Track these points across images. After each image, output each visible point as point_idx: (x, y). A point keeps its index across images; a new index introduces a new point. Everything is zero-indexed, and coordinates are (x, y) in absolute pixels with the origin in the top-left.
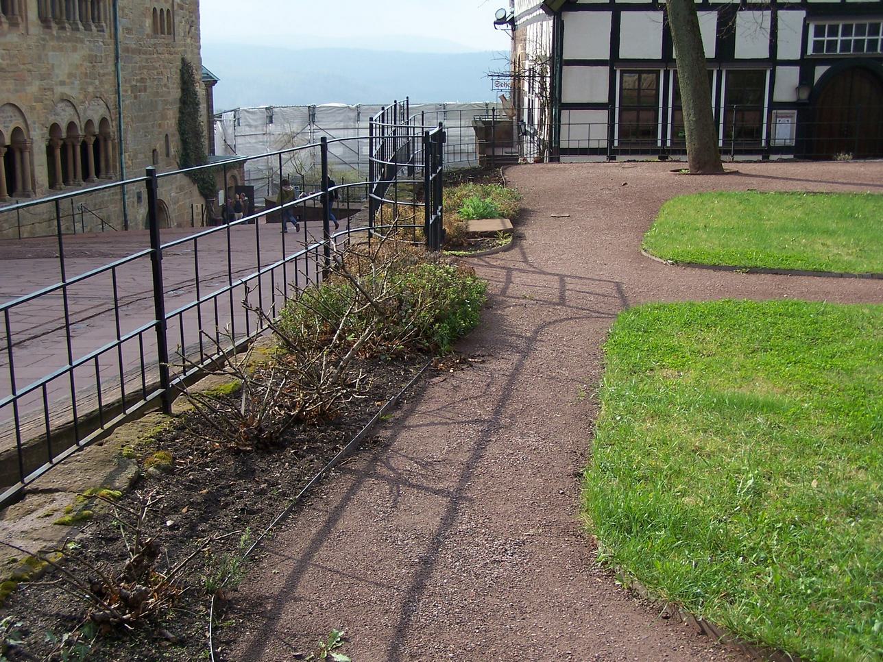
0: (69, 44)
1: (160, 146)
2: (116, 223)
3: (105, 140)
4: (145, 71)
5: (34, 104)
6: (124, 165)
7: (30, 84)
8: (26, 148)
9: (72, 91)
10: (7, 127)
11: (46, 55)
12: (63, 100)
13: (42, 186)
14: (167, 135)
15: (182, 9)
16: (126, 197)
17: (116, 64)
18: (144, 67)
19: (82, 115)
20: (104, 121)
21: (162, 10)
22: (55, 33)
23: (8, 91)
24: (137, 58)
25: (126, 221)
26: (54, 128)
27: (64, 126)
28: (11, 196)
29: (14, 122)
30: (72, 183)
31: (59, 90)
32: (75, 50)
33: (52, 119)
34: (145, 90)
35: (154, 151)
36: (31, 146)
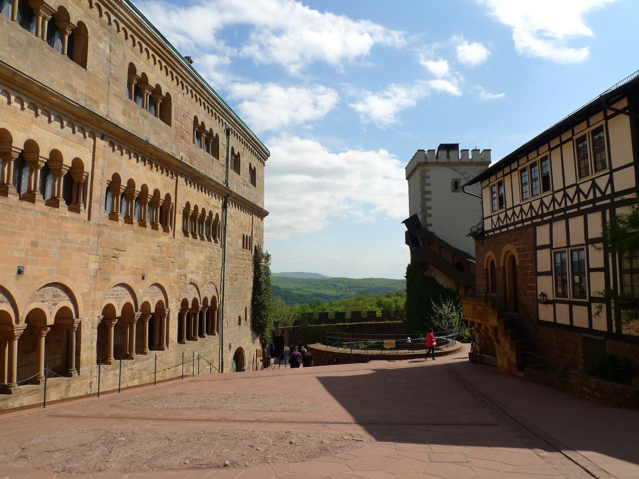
0: (199, 248)
2: (216, 364)
5: (174, 285)
7: (173, 271)
9: (197, 278)
10: (154, 300)
11: (184, 253)
12: (191, 283)
13: (173, 341)
15: (256, 237)
16: (224, 346)
21: (247, 236)
22: (190, 239)
23: (157, 274)
28: (150, 350)
29: (158, 296)
31: (189, 276)
32: (201, 252)
33: (184, 296)
34: (237, 280)
35: (240, 318)
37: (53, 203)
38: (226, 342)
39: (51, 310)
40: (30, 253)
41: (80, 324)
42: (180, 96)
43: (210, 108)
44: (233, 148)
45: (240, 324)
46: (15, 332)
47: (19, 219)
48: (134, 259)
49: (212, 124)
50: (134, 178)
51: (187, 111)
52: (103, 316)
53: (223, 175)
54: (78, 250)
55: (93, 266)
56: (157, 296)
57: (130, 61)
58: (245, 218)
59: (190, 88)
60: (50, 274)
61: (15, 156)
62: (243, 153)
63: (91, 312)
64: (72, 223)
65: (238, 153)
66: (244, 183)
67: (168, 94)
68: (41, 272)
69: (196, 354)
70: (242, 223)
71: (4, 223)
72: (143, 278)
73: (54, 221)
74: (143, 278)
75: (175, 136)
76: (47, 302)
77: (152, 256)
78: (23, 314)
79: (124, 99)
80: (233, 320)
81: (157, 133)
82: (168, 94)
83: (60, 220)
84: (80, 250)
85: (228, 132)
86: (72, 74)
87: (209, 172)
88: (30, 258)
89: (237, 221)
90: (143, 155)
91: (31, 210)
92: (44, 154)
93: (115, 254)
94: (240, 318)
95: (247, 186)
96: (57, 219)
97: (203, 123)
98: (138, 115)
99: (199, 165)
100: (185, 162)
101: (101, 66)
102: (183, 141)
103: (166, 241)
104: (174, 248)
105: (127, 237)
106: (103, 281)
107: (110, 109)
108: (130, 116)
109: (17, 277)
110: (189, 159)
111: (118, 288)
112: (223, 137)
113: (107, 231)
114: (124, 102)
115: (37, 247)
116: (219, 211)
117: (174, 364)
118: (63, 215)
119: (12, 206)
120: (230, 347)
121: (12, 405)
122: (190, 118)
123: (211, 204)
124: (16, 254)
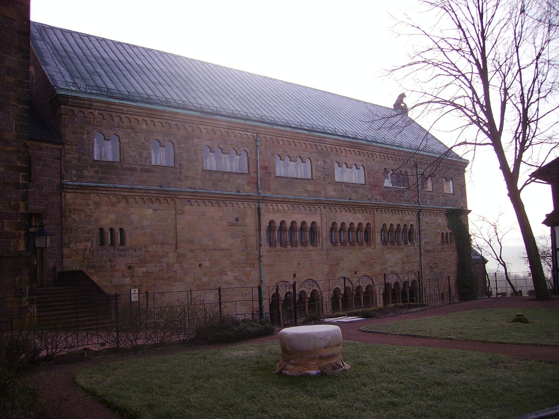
9: (397, 269)
17: (420, 258)
18: (436, 258)
20: (414, 282)
31: (390, 269)
50: (344, 221)
55: (326, 270)
68: (302, 276)
72: (355, 273)
74: (355, 273)
116: (414, 223)
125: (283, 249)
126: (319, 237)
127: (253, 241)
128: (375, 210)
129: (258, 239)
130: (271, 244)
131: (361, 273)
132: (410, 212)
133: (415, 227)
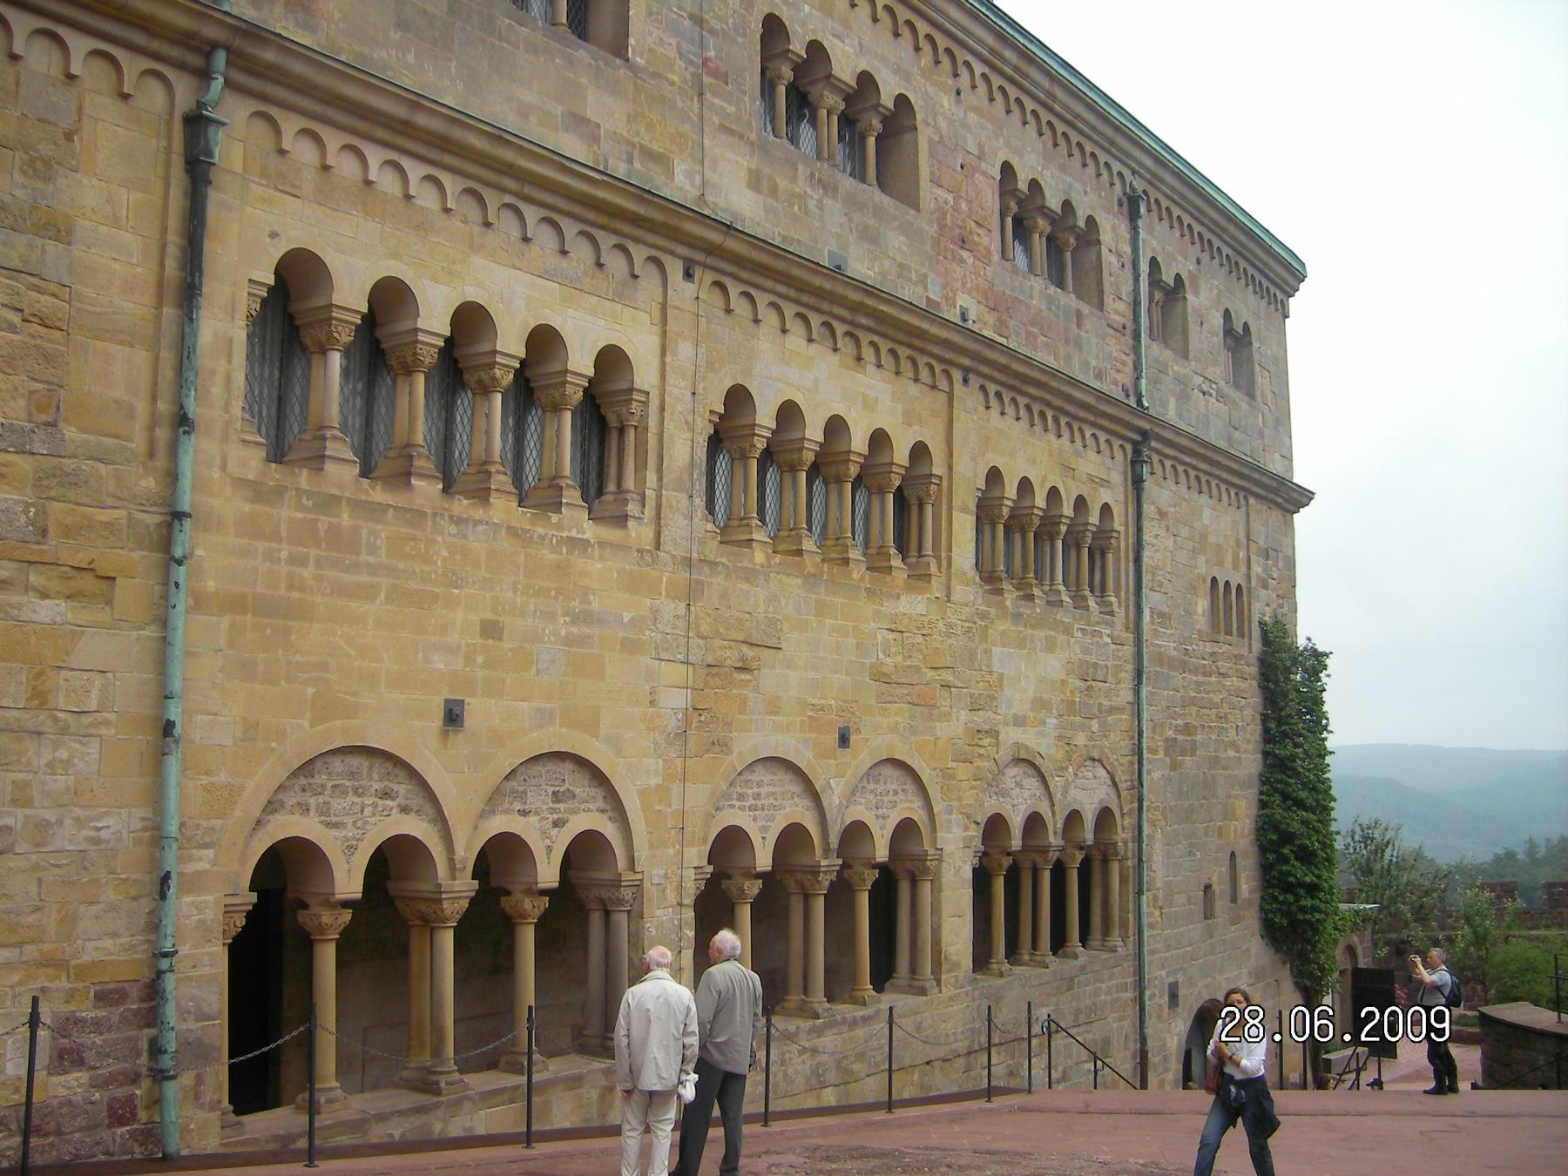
0: (1040, 634)
1: (1218, 876)
2: (1123, 1059)
3: (1105, 861)
4: (1194, 710)
6: (1145, 921)
7: (947, 717)
8: (926, 870)
9: (1041, 742)
10: (884, 818)
12: (1018, 761)
13: (957, 965)
14: (1233, 853)
15: (1266, 587)
16: (1147, 994)
17: (1137, 690)
19: (1058, 797)
20: (1105, 816)
21: (1227, 584)
23: (894, 729)
24: (1178, 678)
25: (1143, 1055)
26: (995, 826)
27: (1016, 822)
29: (900, 807)
30: (1026, 957)
31: (1011, 735)
32: (1050, 646)
33: (991, 805)
35: (1207, 888)
36: (938, 867)
37: (538, 496)
38: (1158, 976)
39: (548, 842)
40: (480, 659)
41: (638, 887)
42: (946, 101)
43: (1060, 127)
44: (1154, 263)
45: (1208, 914)
46: (445, 905)
47: (445, 554)
48: (811, 674)
49: (1062, 183)
50: (799, 398)
51: (974, 149)
52: (710, 869)
53: (1124, 364)
54: (622, 645)
55: (675, 701)
56: (894, 804)
57: (766, 11)
58: (1216, 518)
59: (979, 68)
60: (540, 726)
61: (429, 357)
62: (1194, 279)
63: (671, 851)
64: (602, 558)
65: (1178, 277)
66: (1205, 388)
67: (902, 101)
68: (511, 722)
69: (1041, 1013)
70: (1204, 537)
71: (401, 566)
72: (844, 740)
73: (549, 556)
74: (844, 740)
75: (936, 243)
76: (537, 813)
77: (872, 666)
78: (467, 852)
79: (753, 136)
80: (1180, 899)
81: (870, 237)
82: (902, 101)
83: (564, 550)
84: (631, 647)
85: (1131, 206)
86: (584, 81)
87: (1068, 358)
88: (481, 673)
89: (1184, 532)
90: (824, 318)
91: (477, 523)
92: (510, 343)
93: (743, 659)
94: (1207, 888)
95: (1221, 396)
96: (555, 549)
97: (1034, 184)
98: (802, 186)
99: (1028, 333)
100: (975, 328)
101: (674, 42)
102: (965, 254)
103: (921, 608)
104: (949, 635)
105: (783, 602)
106: (707, 751)
107: (709, 174)
108: (774, 191)
109: (445, 734)
110: (991, 319)
111: (760, 774)
112: (1113, 228)
113: (718, 581)
114: (752, 144)
115: (500, 639)
116: (1114, 495)
117: (961, 1046)
118: (574, 533)
119: (423, 514)
120: (1174, 997)
121: (442, 1131)
122: (984, 173)
123: (1083, 472)
124: (439, 663)
125: (379, 495)
126: (641, 466)
127: (119, 375)
128: (957, 376)
129: (167, 374)
130: (284, 433)
131: (882, 735)
132: (1103, 437)
133: (1118, 524)
